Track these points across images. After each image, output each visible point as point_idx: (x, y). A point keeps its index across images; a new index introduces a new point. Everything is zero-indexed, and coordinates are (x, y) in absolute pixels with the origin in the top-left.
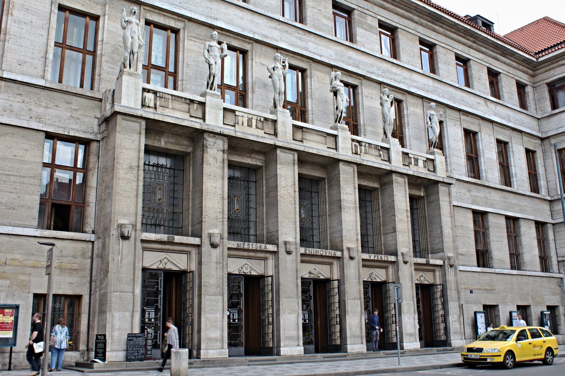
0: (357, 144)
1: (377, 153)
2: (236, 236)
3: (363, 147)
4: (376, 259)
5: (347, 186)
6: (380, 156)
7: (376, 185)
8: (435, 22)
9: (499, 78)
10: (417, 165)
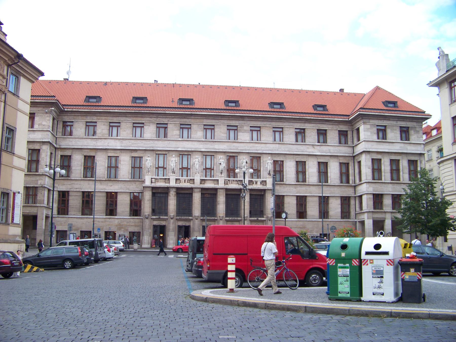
1: (237, 183)
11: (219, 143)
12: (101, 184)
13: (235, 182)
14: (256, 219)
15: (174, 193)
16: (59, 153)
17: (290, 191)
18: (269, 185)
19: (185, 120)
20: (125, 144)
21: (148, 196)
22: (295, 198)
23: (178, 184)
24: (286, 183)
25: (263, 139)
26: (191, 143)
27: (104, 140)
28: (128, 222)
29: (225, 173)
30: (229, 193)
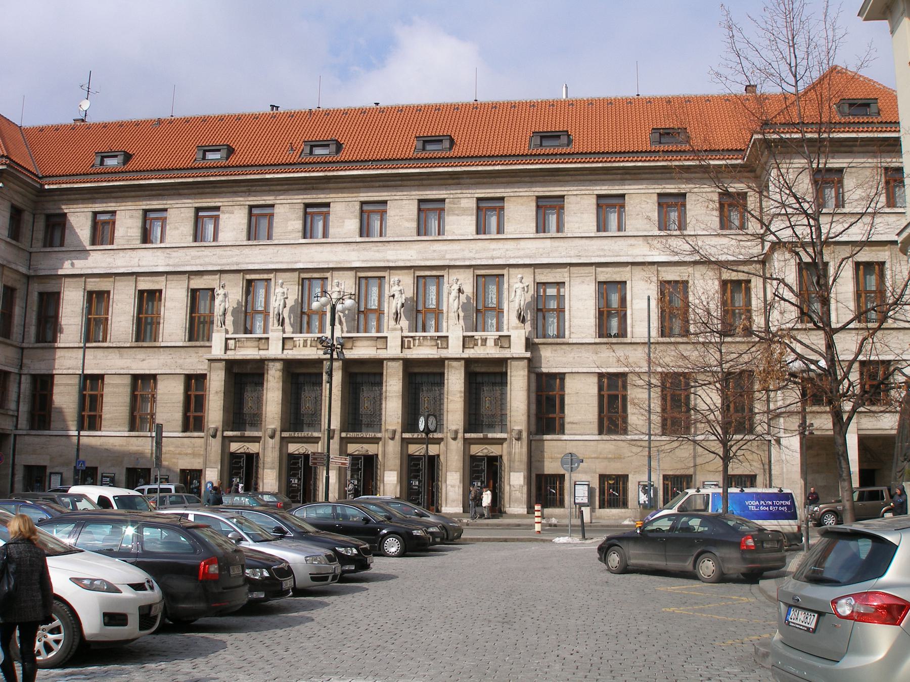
1: (434, 343)
6: (437, 345)
11: (397, 245)
12: (121, 356)
13: (429, 343)
14: (481, 435)
15: (278, 374)
16: (36, 289)
17: (579, 365)
18: (518, 349)
20: (177, 260)
21: (216, 383)
22: (595, 380)
23: (290, 352)
24: (571, 341)
25: (510, 229)
27: (129, 252)
28: (177, 447)
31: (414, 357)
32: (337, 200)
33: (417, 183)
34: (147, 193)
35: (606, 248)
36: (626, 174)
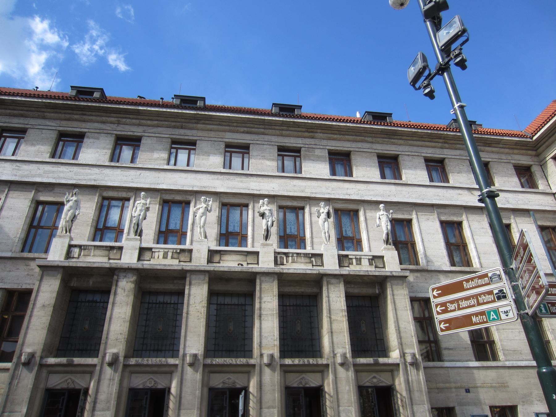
0: (283, 256)
1: (307, 260)
2: (159, 353)
3: (290, 258)
4: (301, 363)
5: (266, 295)
6: (311, 262)
7: (315, 290)
8: (392, 137)
9: (489, 166)
10: (360, 264)
11: (260, 179)
13: (303, 260)
14: (370, 360)
19: (182, 131)
20: (26, 173)
26: (193, 175)
29: (274, 239)
30: (288, 290)
31: (291, 271)
32: (203, 138)
33: (278, 132)
34: (8, 111)
35: (440, 194)
36: (445, 143)
